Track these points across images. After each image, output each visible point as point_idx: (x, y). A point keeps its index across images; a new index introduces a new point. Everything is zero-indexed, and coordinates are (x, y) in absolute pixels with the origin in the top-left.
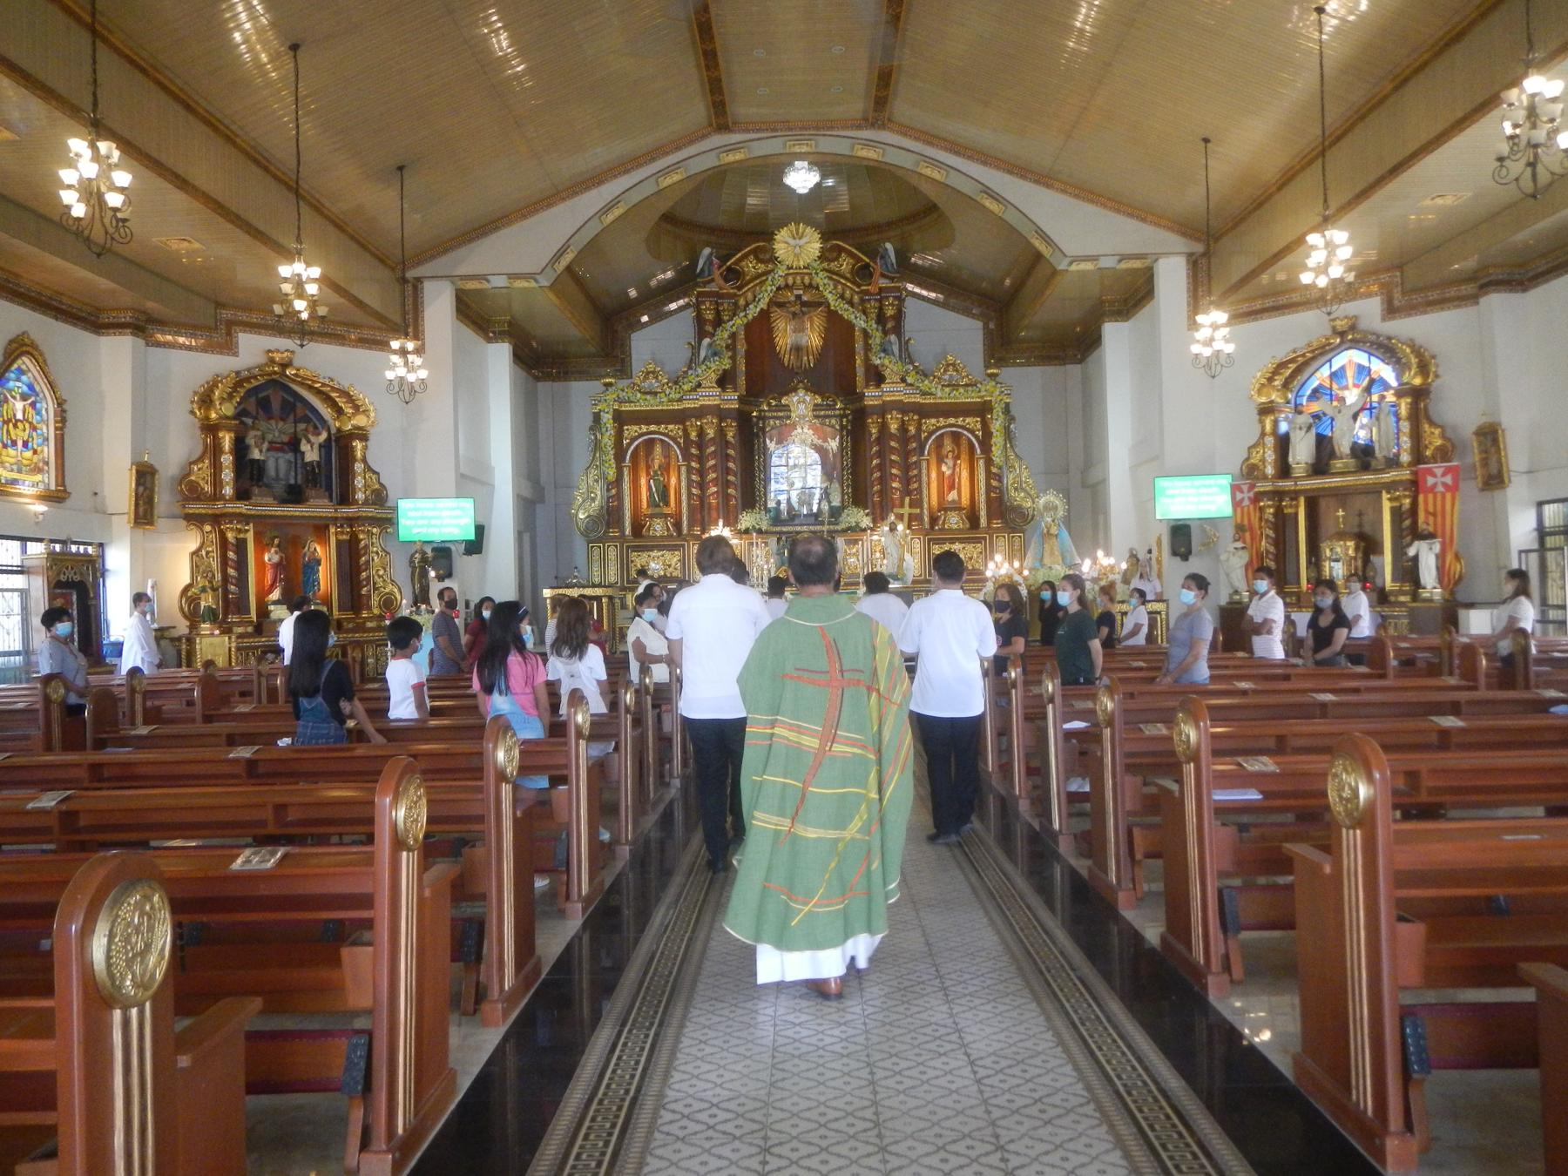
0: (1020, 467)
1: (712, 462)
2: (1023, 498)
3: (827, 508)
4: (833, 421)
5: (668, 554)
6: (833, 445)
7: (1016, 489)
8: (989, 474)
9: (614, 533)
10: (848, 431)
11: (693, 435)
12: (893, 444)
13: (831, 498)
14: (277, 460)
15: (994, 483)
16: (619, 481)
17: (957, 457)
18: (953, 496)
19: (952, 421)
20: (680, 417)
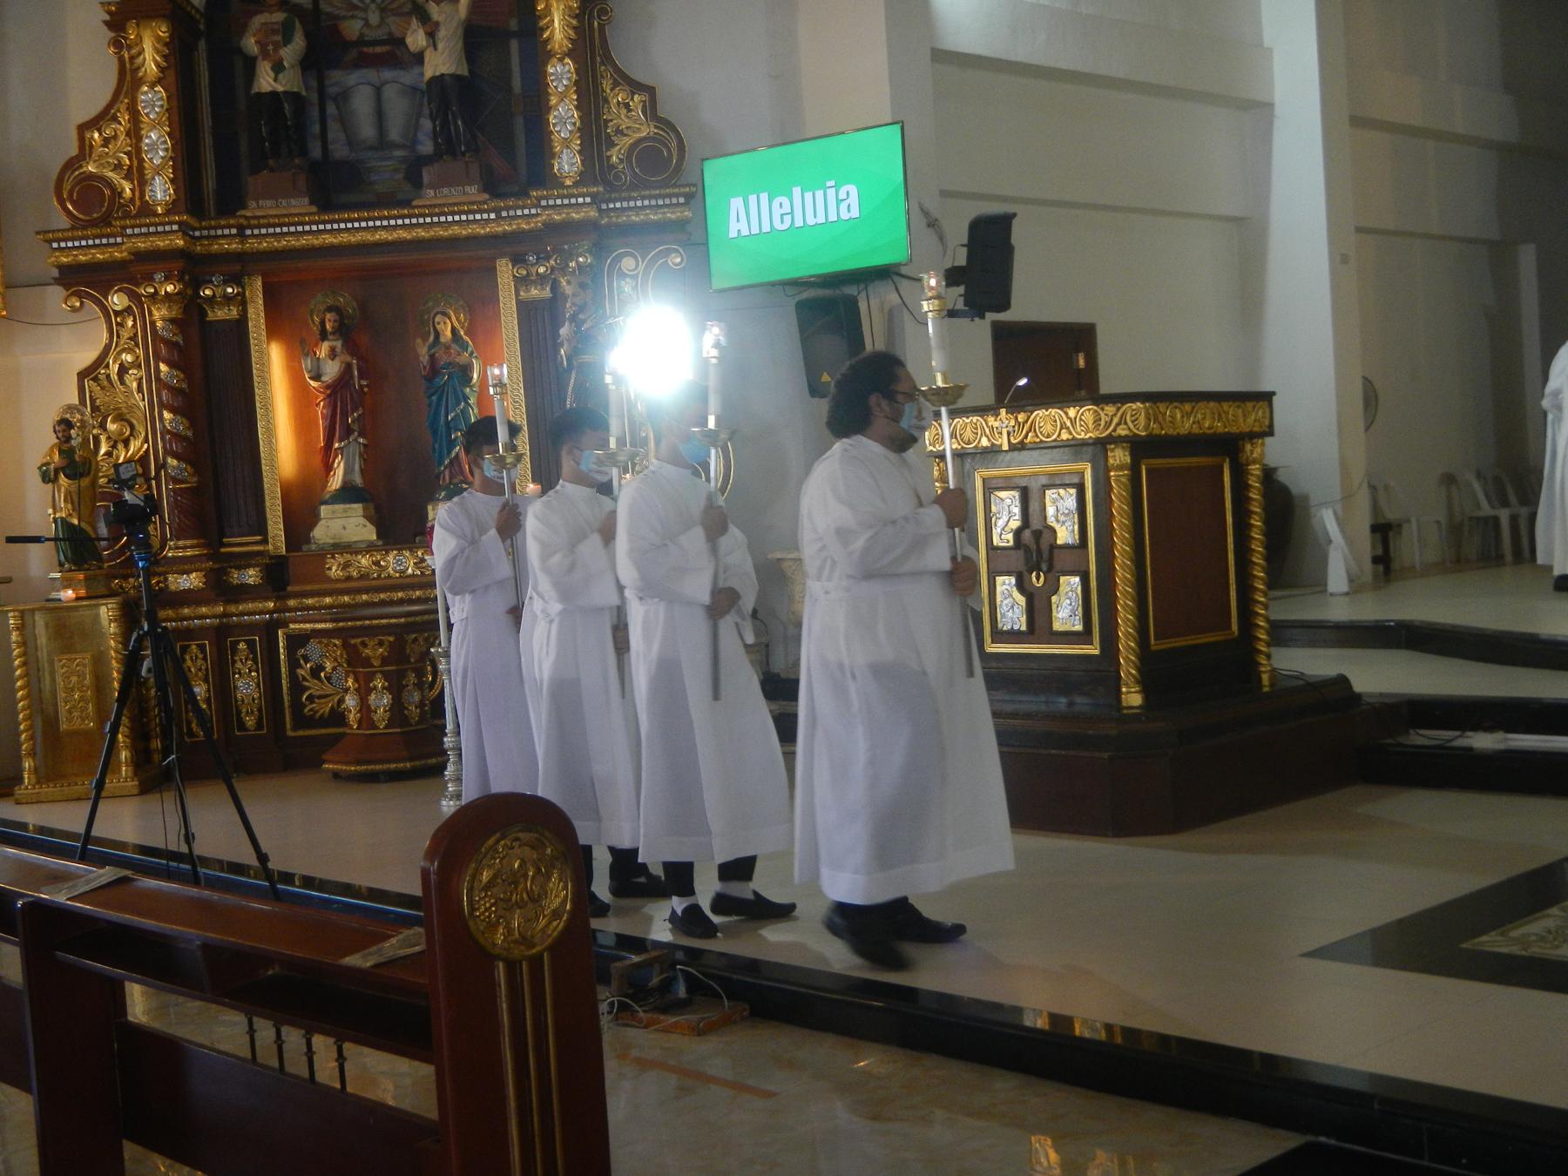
14: (378, 90)
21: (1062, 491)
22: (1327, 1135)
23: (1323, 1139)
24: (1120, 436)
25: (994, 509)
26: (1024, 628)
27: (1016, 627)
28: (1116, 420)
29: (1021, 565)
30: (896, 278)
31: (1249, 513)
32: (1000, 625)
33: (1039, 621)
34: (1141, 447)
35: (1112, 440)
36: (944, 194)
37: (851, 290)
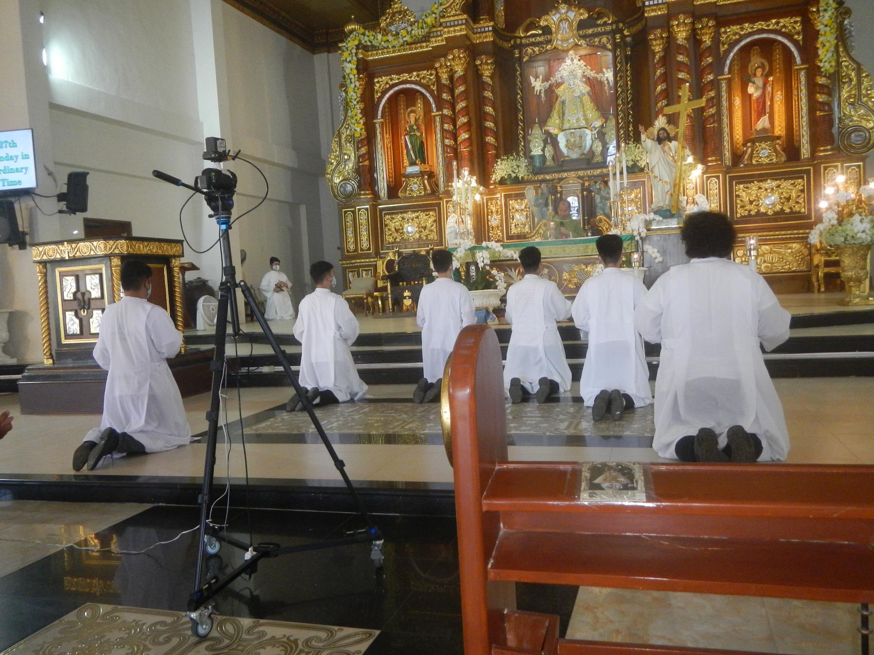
0: (859, 70)
1: (461, 105)
2: (861, 117)
3: (600, 149)
4: (604, 40)
5: (422, 215)
6: (609, 75)
7: (852, 104)
8: (813, 88)
9: (366, 196)
10: (626, 57)
11: (444, 77)
12: (680, 58)
13: (607, 138)
15: (821, 98)
16: (370, 139)
17: (770, 74)
18: (763, 123)
19: (758, 26)
20: (426, 61)
21: (93, 276)
22: (162, 502)
23: (160, 504)
24: (115, 253)
25: (64, 284)
26: (78, 333)
27: (75, 333)
28: (114, 247)
29: (76, 307)
30: (34, 196)
31: (175, 287)
32: (68, 332)
33: (84, 329)
34: (123, 258)
35: (115, 255)
36: (56, 163)
37: (13, 200)
